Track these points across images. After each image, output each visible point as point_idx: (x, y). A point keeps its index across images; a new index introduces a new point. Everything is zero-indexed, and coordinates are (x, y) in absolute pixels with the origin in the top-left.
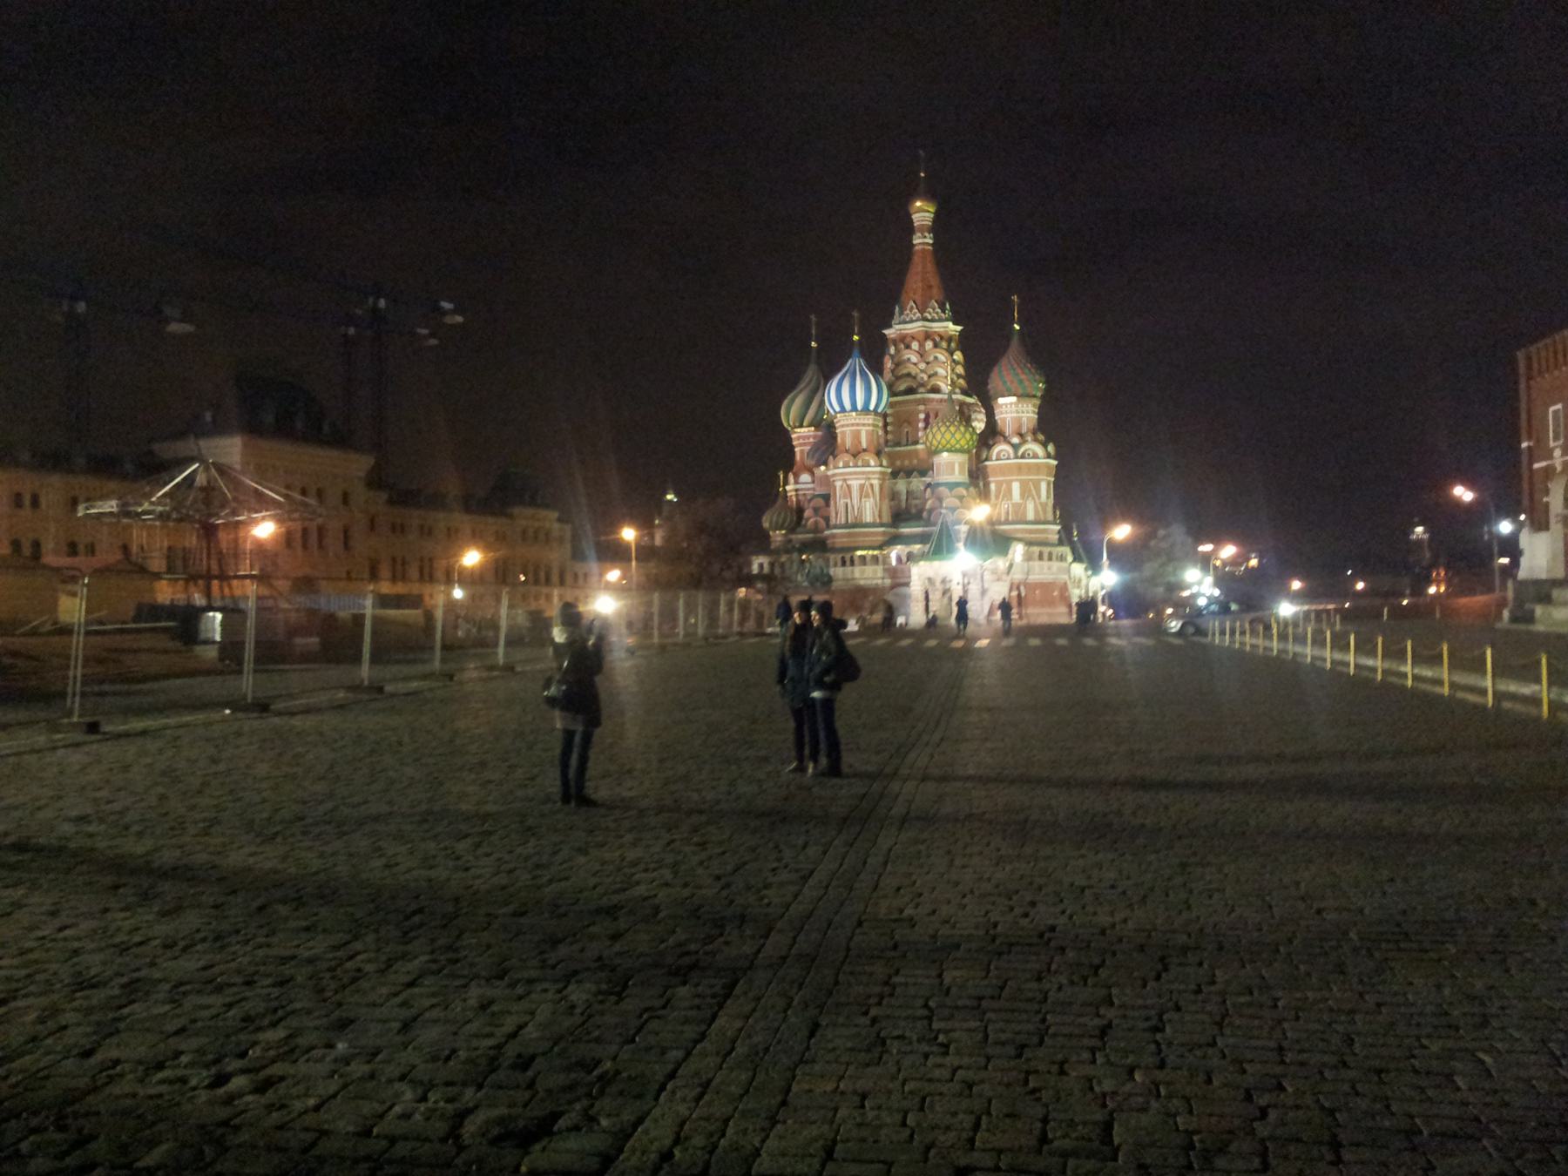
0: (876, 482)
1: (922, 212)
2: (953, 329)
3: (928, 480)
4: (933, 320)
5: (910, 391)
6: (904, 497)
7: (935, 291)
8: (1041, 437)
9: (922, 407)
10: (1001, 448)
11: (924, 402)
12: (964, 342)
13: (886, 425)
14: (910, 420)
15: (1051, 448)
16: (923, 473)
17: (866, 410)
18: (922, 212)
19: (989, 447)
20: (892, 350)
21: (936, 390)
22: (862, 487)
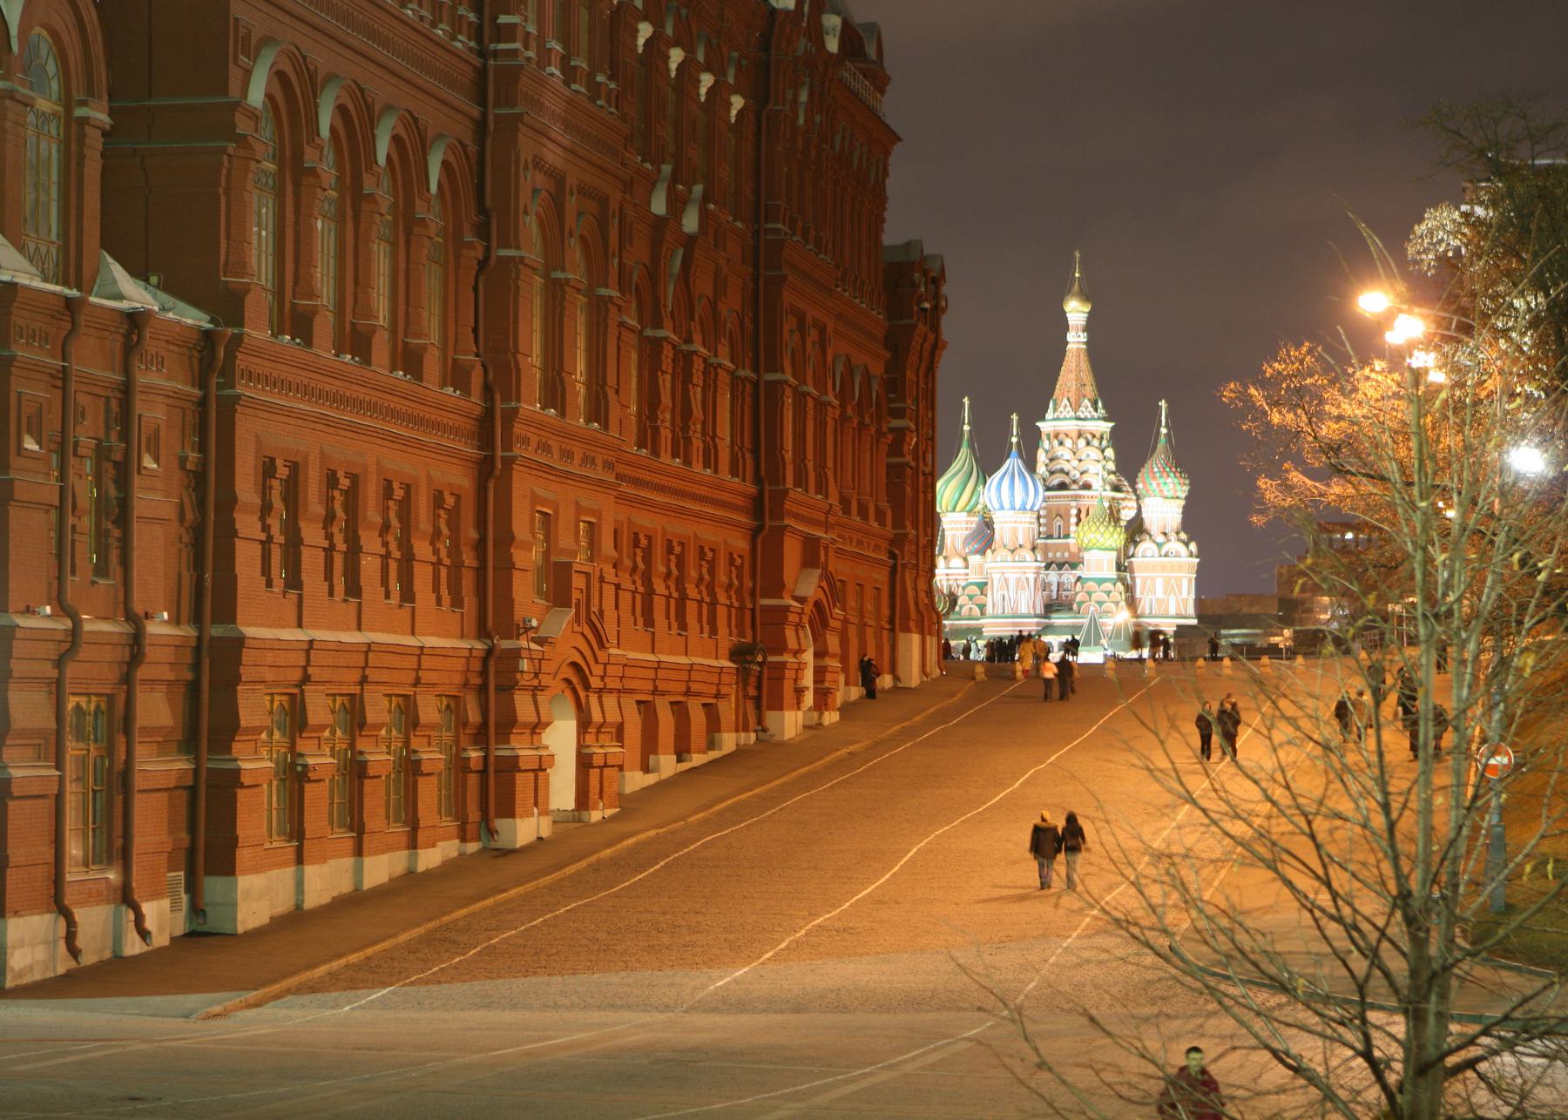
0: (1032, 577)
1: (1076, 311)
2: (1106, 427)
3: (1078, 573)
4: (1085, 419)
5: (1063, 486)
6: (1054, 588)
7: (1090, 390)
8: (1183, 536)
9: (1073, 503)
10: (1145, 547)
11: (1076, 498)
12: (1116, 438)
13: (1039, 518)
14: (1062, 514)
15: (1193, 546)
16: (1073, 566)
17: (1023, 508)
18: (1076, 311)
19: (1136, 544)
20: (1046, 444)
21: (1087, 486)
22: (1018, 580)
